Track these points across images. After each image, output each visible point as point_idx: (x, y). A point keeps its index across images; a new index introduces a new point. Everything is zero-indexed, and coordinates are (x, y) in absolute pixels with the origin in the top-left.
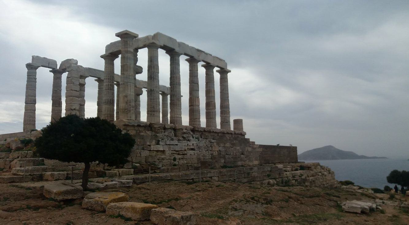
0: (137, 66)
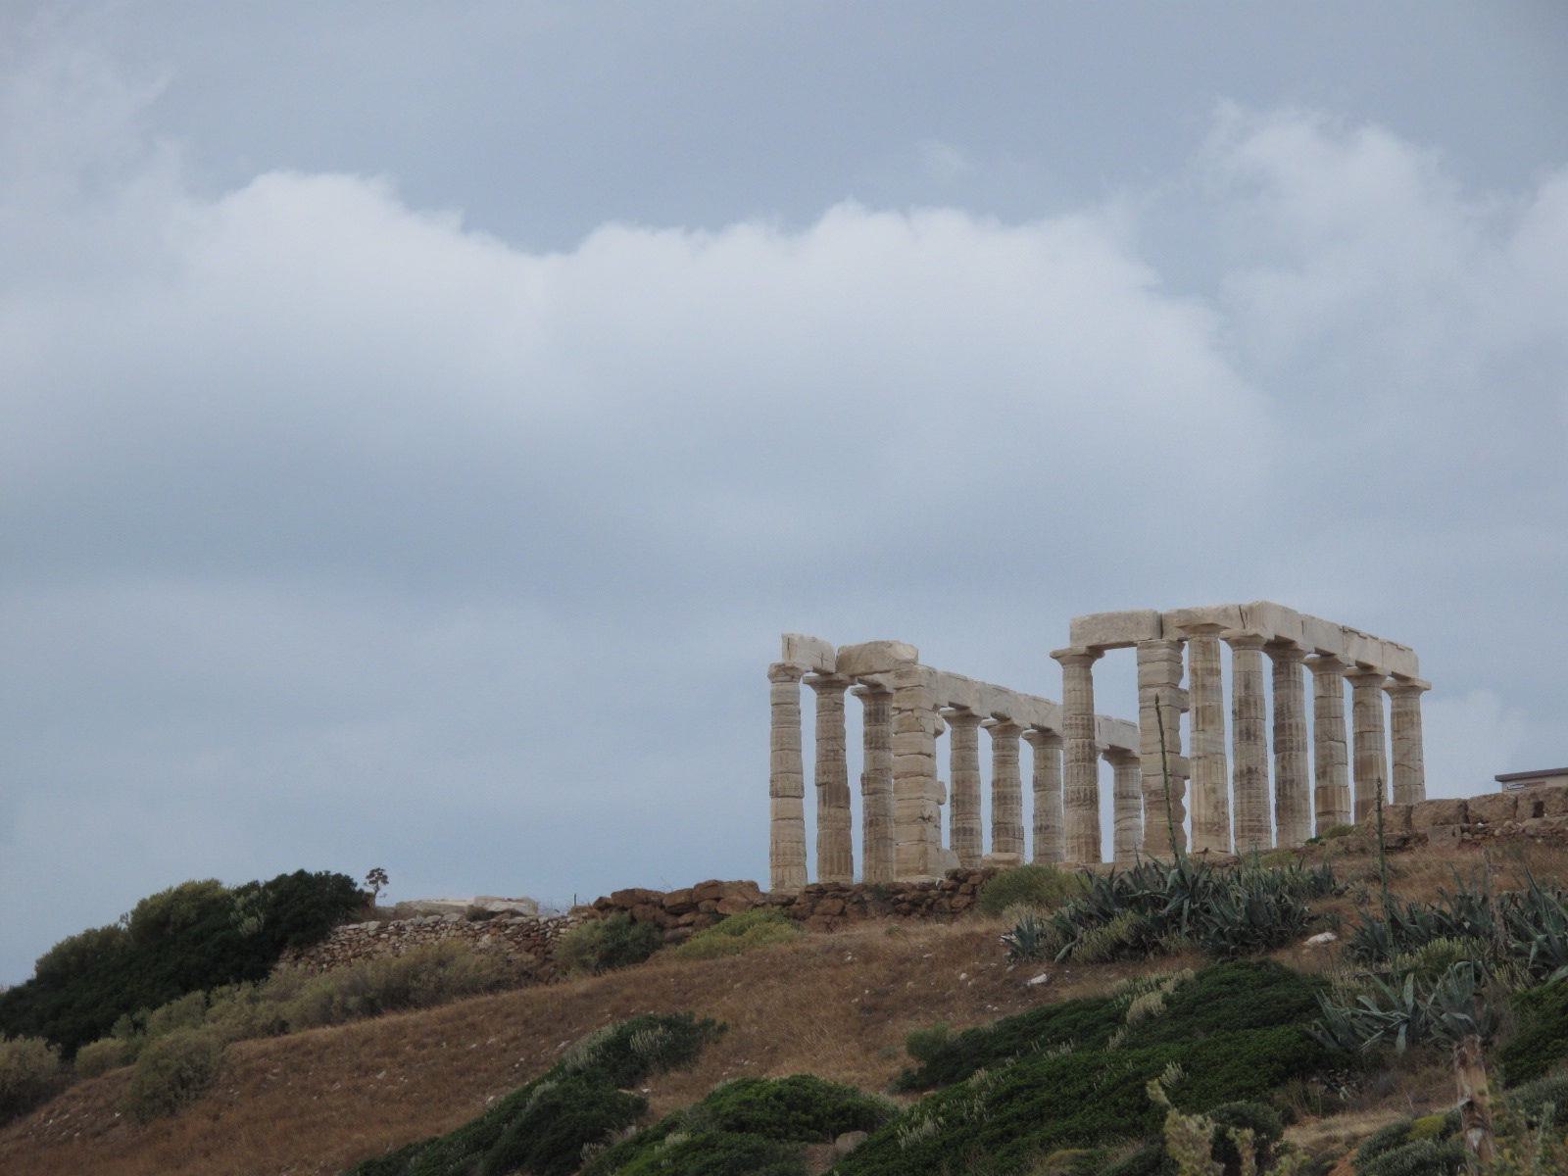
0: (1179, 689)
